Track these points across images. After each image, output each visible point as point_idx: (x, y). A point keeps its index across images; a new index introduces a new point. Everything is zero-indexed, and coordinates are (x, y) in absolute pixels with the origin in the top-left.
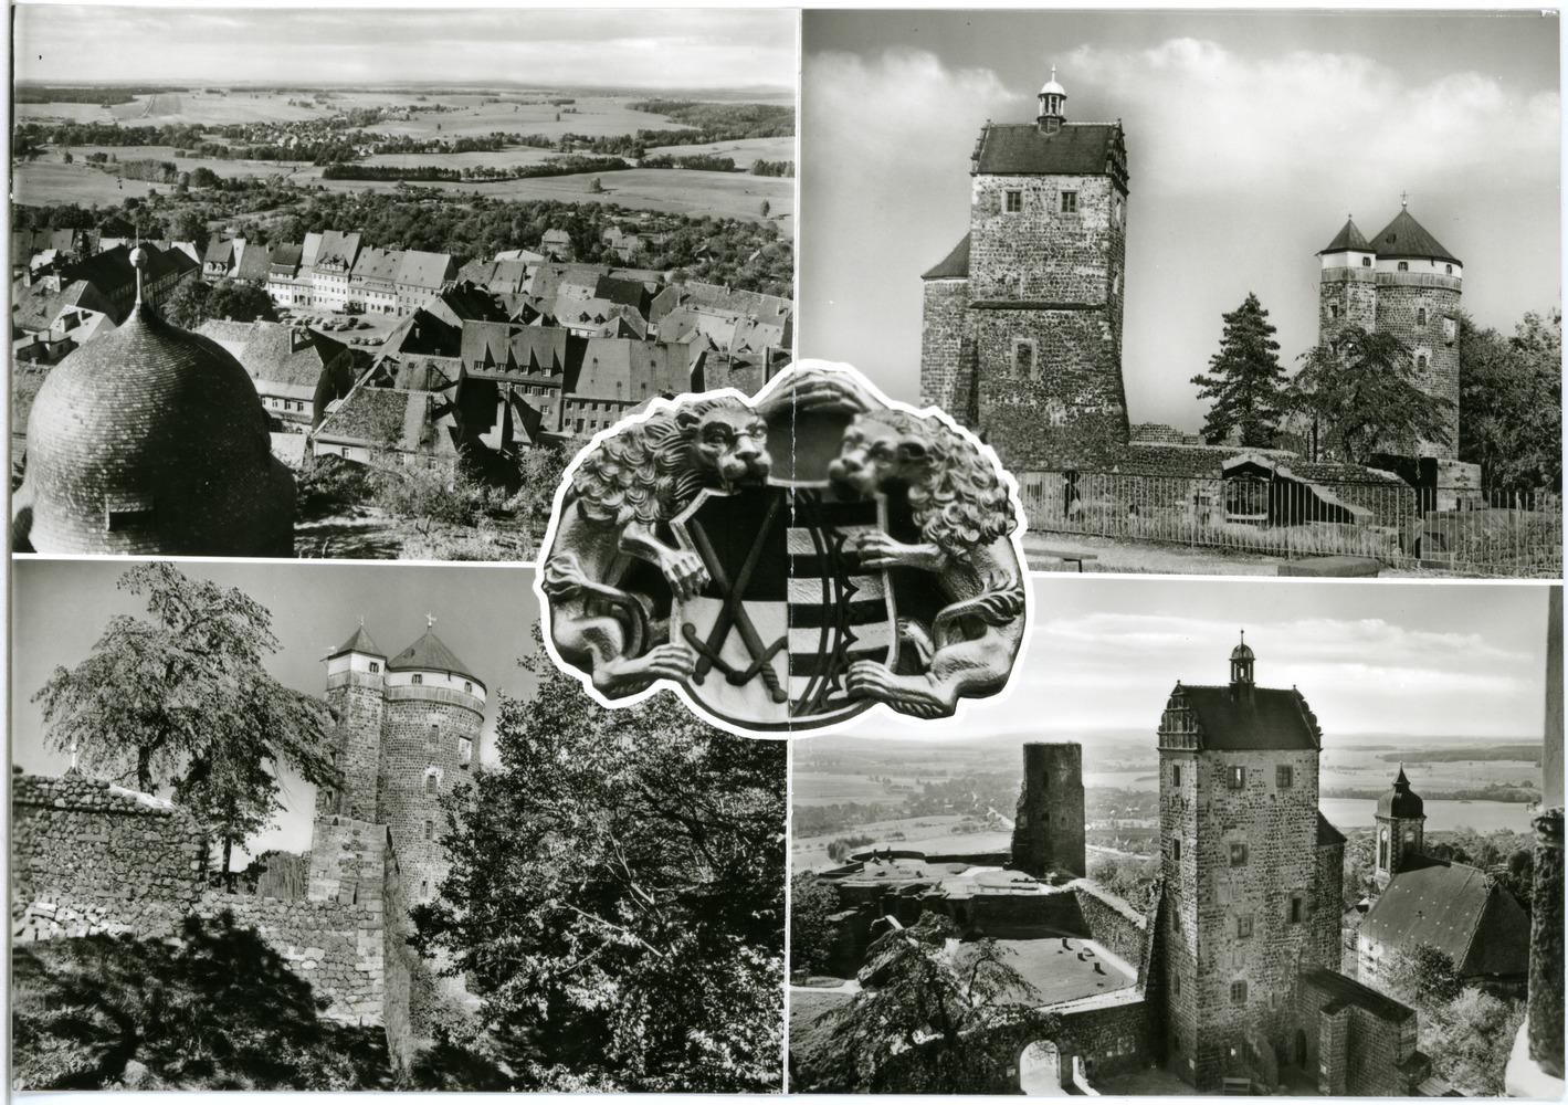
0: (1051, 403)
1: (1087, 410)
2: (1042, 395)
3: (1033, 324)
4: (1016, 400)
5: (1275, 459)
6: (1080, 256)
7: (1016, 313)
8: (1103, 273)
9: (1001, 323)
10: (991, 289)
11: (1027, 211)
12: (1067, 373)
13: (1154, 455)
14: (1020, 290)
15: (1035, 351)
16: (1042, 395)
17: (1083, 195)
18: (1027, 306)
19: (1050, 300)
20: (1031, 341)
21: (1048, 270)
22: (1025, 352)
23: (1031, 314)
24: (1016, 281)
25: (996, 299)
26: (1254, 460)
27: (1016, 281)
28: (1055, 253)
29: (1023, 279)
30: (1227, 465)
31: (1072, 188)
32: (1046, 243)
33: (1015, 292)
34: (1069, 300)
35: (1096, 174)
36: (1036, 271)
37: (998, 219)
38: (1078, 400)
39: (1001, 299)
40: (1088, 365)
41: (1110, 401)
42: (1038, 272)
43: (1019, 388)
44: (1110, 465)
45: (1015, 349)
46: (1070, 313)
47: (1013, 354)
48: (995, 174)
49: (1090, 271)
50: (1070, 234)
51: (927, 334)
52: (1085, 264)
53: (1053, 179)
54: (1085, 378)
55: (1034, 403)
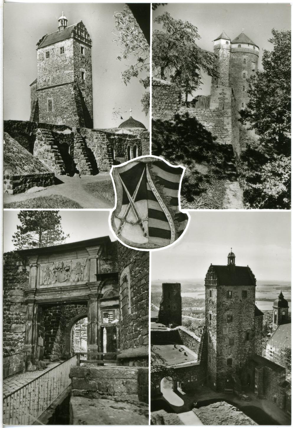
0: (59, 118)
1: (68, 120)
3: (52, 93)
4: (49, 119)
6: (65, 67)
8: (73, 71)
9: (44, 94)
11: (51, 56)
15: (53, 101)
17: (66, 47)
20: (52, 99)
21: (57, 74)
22: (50, 102)
23: (51, 90)
24: (49, 80)
25: (44, 87)
27: (49, 80)
31: (63, 46)
32: (56, 66)
33: (49, 84)
34: (63, 83)
36: (54, 75)
37: (44, 61)
38: (65, 117)
40: (68, 104)
41: (75, 115)
42: (54, 76)
45: (48, 102)
47: (47, 104)
49: (69, 72)
52: (67, 69)
54: (67, 108)
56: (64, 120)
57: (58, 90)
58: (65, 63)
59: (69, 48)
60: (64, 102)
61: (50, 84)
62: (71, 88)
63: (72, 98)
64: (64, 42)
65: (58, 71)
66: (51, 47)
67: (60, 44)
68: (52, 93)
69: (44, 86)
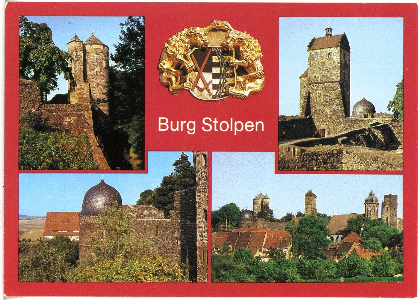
1: (335, 109)
2: (325, 106)
3: (322, 87)
5: (384, 121)
9: (314, 88)
10: (313, 79)
12: (330, 100)
13: (352, 121)
14: (319, 79)
15: (322, 94)
16: (325, 106)
18: (320, 83)
19: (326, 81)
20: (322, 92)
21: (326, 73)
25: (314, 82)
26: (378, 121)
29: (320, 76)
30: (371, 123)
31: (331, 51)
35: (336, 47)
37: (314, 61)
38: (333, 107)
39: (315, 82)
43: (319, 104)
44: (341, 124)
45: (317, 94)
46: (331, 84)
48: (313, 50)
49: (336, 73)
50: (331, 63)
51: (301, 92)
53: (326, 49)
54: (335, 101)
55: (322, 108)
56: (332, 109)
57: (327, 86)
58: (333, 65)
59: (336, 54)
60: (332, 96)
61: (320, 79)
62: (338, 86)
63: (339, 94)
64: (332, 49)
65: (327, 71)
66: (321, 51)
67: (329, 50)
68: (322, 87)
69: (314, 80)
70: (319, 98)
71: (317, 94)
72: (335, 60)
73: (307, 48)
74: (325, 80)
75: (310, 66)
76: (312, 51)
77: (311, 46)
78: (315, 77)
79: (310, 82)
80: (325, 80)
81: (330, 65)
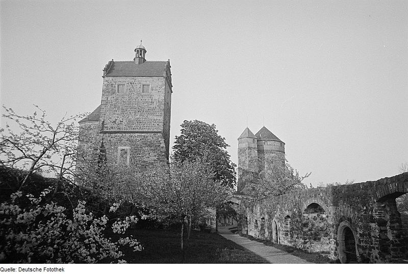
7: (120, 135)
15: (129, 152)
20: (127, 148)
25: (111, 130)
28: (140, 110)
29: (124, 121)
31: (148, 83)
33: (121, 126)
45: (119, 151)
49: (155, 118)
53: (139, 79)
61: (123, 127)
62: (160, 139)
64: (150, 79)
66: (129, 79)
70: (122, 159)
71: (119, 151)
72: (156, 97)
73: (102, 73)
74: (133, 129)
75: (105, 103)
76: (111, 78)
77: (110, 69)
78: (115, 122)
79: (105, 130)
80: (133, 129)
81: (145, 105)
